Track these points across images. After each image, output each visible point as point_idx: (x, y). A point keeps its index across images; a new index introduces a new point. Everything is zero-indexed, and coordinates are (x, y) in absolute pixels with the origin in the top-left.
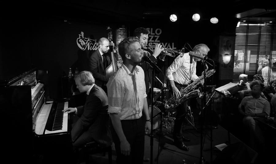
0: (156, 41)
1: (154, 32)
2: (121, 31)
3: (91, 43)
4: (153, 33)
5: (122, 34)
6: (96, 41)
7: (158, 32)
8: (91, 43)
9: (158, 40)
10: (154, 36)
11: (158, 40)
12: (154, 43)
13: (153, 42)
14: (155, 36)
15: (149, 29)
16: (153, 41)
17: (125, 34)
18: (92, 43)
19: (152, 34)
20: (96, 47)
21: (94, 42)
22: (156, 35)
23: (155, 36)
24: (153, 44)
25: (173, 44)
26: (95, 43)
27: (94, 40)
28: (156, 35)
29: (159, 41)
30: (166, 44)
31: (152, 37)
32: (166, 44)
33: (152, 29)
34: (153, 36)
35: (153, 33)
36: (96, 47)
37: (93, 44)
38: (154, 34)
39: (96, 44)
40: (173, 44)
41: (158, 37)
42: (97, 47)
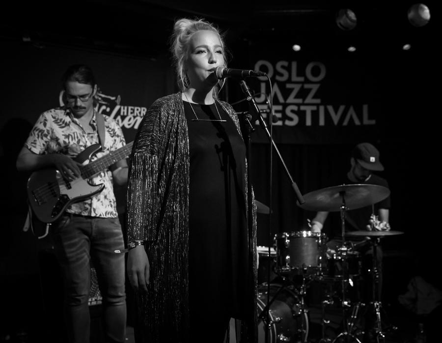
0: (309, 100)
1: (301, 72)
3: (104, 107)
4: (298, 75)
6: (118, 101)
7: (315, 72)
8: (104, 107)
9: (315, 97)
10: (302, 89)
11: (315, 97)
12: (302, 108)
13: (298, 105)
14: (307, 86)
15: (286, 64)
16: (300, 101)
18: (107, 106)
19: (295, 78)
20: (119, 118)
21: (112, 105)
22: (307, 81)
23: (307, 86)
24: (299, 108)
25: (365, 108)
26: (117, 108)
27: (113, 96)
28: (307, 81)
29: (318, 101)
31: (297, 88)
33: (294, 65)
35: (298, 75)
36: (119, 118)
37: (108, 110)
38: (302, 79)
39: (119, 110)
40: (365, 108)
41: (315, 88)
42: (123, 118)
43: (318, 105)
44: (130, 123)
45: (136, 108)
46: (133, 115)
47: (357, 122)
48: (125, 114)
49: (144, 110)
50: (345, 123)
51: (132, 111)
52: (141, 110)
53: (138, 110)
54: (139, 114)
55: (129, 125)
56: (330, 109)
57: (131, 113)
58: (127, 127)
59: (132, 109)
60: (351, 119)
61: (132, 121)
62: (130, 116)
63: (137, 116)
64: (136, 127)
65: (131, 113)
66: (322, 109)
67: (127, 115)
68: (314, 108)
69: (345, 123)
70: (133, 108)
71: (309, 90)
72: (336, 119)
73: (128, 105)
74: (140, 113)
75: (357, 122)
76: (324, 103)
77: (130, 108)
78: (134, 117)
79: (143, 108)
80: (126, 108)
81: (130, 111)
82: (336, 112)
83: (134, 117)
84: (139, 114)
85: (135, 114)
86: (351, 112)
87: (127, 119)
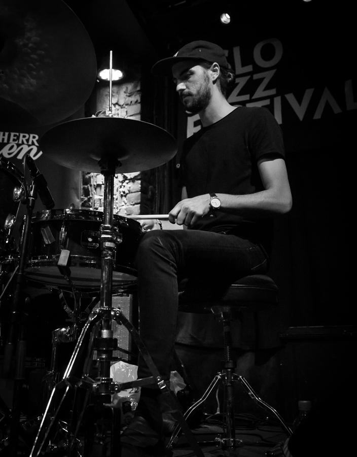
0: (259, 93)
1: (247, 59)
2: (118, 93)
4: (244, 64)
5: (121, 102)
7: (267, 54)
9: (268, 88)
10: (251, 78)
11: (268, 88)
17: (133, 99)
19: (240, 70)
22: (257, 69)
23: (256, 77)
28: (257, 69)
29: (273, 92)
30: (308, 94)
31: (242, 82)
32: (308, 94)
34: (248, 78)
35: (244, 64)
38: (249, 68)
41: (268, 76)
43: (271, 98)
44: (11, 151)
45: (22, 135)
46: (17, 142)
47: (337, 110)
48: (6, 141)
49: (34, 137)
50: (318, 116)
51: (15, 138)
52: (29, 136)
53: (24, 137)
54: (25, 142)
55: (9, 154)
56: (290, 98)
57: (14, 140)
58: (8, 156)
59: (15, 136)
60: (328, 107)
61: (15, 150)
62: (12, 143)
63: (23, 143)
64: (20, 157)
65: (14, 140)
66: (278, 101)
67: (8, 142)
68: (267, 102)
69: (318, 116)
70: (18, 134)
71: (261, 80)
72: (300, 111)
73: (10, 132)
74: (28, 140)
75: (337, 110)
76: (281, 93)
77: (12, 134)
78: (18, 145)
79: (32, 136)
80: (7, 134)
81: (12, 138)
82: (300, 102)
83: (18, 145)
84: (25, 142)
85: (20, 142)
86: (327, 96)
87: (9, 146)
